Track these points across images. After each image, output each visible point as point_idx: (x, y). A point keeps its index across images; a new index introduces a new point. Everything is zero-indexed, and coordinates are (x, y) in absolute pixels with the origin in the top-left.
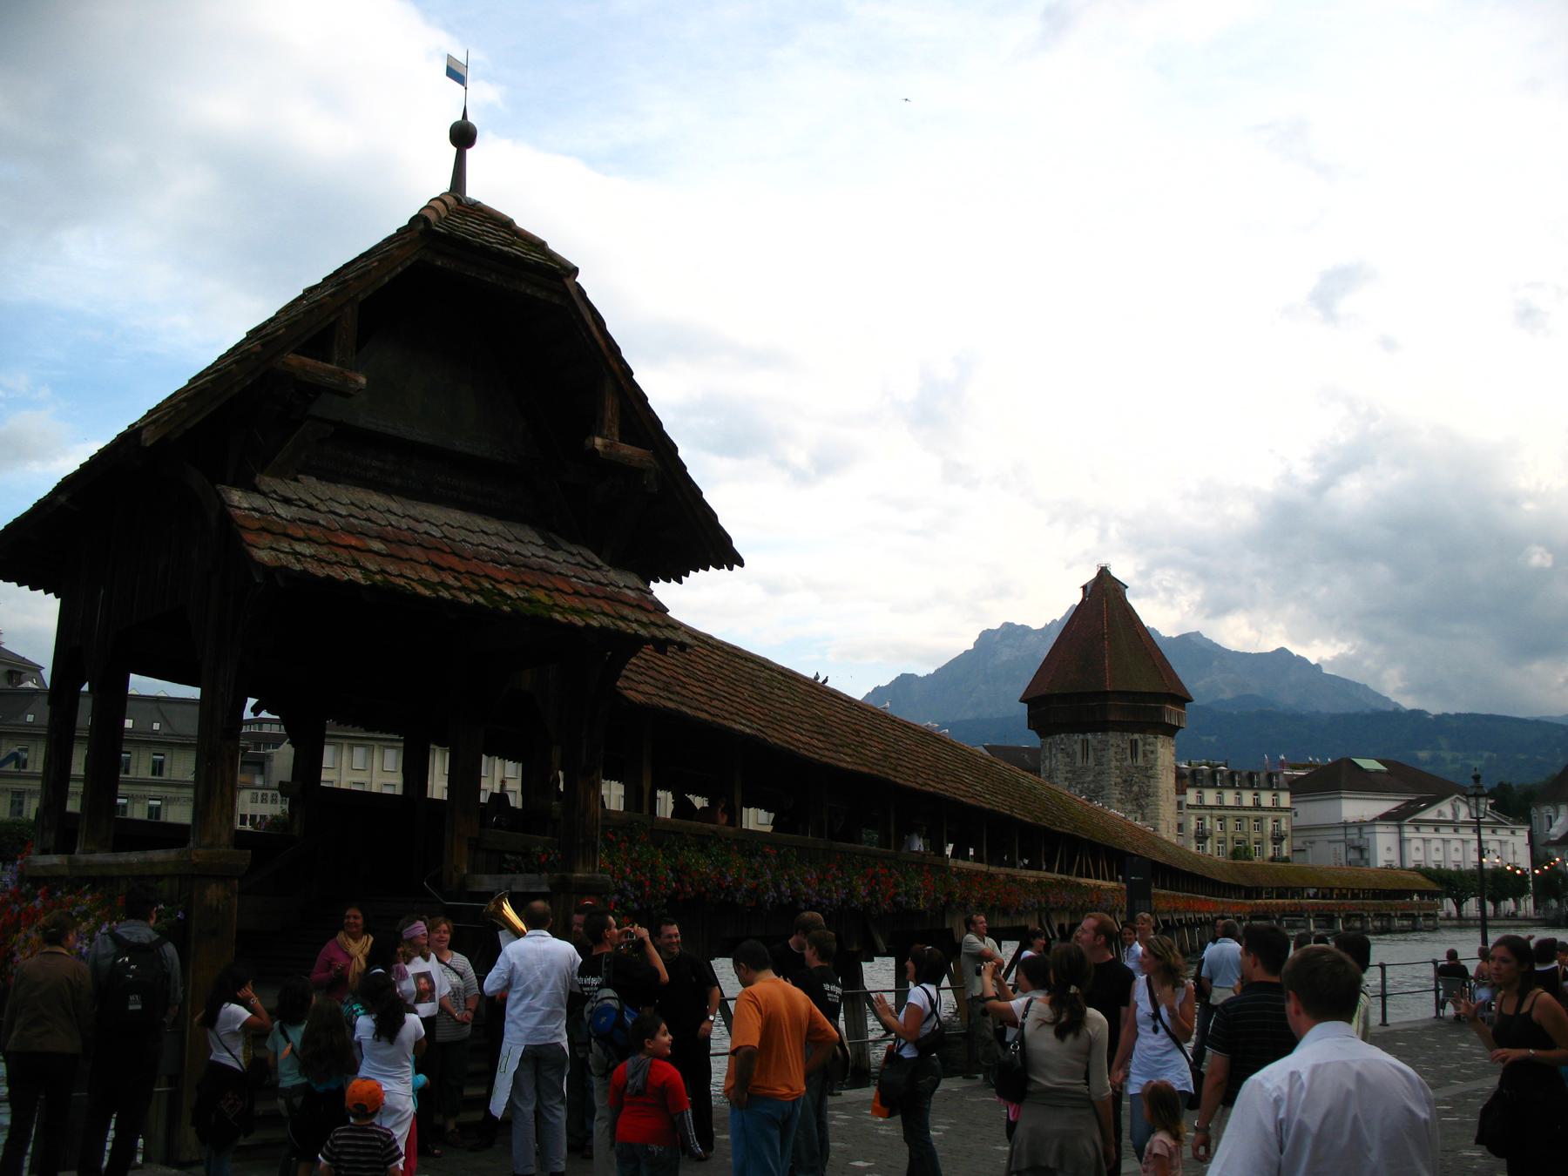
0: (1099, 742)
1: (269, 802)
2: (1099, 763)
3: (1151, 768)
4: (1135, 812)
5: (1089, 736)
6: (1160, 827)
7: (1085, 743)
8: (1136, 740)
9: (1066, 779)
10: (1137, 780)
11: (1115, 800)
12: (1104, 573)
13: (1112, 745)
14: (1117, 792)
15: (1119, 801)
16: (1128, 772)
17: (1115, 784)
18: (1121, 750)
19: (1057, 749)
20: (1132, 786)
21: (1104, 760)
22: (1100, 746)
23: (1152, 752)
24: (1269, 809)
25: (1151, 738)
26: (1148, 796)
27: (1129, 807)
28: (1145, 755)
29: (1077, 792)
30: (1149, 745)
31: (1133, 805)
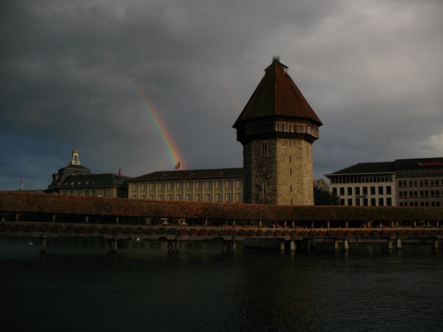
4: (265, 182)
6: (278, 189)
8: (266, 143)
11: (254, 177)
12: (276, 62)
14: (255, 172)
15: (256, 176)
17: (254, 167)
18: (257, 150)
23: (274, 149)
25: (273, 141)
26: (271, 172)
27: (261, 179)
28: (270, 151)
30: (272, 145)
31: (263, 178)
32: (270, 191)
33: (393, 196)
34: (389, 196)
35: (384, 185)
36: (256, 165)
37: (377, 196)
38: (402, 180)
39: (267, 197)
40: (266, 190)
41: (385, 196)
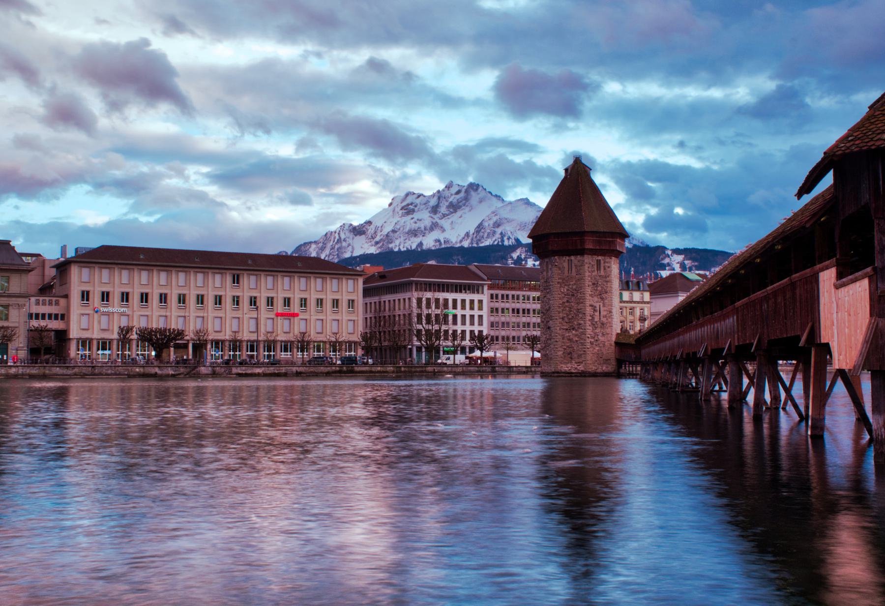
0: (579, 261)
1: (41, 304)
2: (578, 273)
3: (608, 276)
5: (573, 258)
7: (570, 261)
9: (558, 283)
10: (600, 283)
13: (587, 263)
15: (590, 295)
16: (595, 279)
19: (552, 266)
20: (597, 286)
21: (581, 271)
22: (579, 264)
23: (609, 267)
24: (638, 302)
25: (608, 260)
26: (606, 292)
27: (596, 299)
28: (605, 269)
29: (565, 290)
32: (605, 313)
33: (485, 312)
34: (480, 313)
35: (476, 297)
36: (590, 283)
37: (468, 312)
38: (494, 292)
39: (602, 319)
40: (601, 311)
41: (476, 312)
